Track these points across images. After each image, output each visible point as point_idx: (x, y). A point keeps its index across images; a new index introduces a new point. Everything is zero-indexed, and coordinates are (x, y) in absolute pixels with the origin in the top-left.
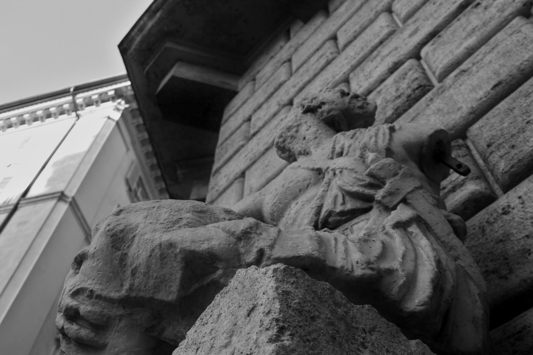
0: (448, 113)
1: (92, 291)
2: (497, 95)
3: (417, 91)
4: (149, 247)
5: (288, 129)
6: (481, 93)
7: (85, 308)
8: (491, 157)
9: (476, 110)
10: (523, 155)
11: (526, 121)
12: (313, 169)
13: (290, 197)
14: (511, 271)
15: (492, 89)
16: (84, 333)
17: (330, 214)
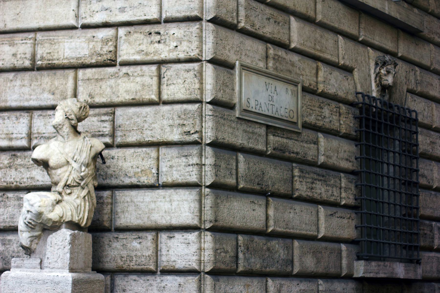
0: (114, 93)
3: (109, 61)
7: (33, 223)
14: (106, 179)
16: (32, 227)
17: (70, 184)
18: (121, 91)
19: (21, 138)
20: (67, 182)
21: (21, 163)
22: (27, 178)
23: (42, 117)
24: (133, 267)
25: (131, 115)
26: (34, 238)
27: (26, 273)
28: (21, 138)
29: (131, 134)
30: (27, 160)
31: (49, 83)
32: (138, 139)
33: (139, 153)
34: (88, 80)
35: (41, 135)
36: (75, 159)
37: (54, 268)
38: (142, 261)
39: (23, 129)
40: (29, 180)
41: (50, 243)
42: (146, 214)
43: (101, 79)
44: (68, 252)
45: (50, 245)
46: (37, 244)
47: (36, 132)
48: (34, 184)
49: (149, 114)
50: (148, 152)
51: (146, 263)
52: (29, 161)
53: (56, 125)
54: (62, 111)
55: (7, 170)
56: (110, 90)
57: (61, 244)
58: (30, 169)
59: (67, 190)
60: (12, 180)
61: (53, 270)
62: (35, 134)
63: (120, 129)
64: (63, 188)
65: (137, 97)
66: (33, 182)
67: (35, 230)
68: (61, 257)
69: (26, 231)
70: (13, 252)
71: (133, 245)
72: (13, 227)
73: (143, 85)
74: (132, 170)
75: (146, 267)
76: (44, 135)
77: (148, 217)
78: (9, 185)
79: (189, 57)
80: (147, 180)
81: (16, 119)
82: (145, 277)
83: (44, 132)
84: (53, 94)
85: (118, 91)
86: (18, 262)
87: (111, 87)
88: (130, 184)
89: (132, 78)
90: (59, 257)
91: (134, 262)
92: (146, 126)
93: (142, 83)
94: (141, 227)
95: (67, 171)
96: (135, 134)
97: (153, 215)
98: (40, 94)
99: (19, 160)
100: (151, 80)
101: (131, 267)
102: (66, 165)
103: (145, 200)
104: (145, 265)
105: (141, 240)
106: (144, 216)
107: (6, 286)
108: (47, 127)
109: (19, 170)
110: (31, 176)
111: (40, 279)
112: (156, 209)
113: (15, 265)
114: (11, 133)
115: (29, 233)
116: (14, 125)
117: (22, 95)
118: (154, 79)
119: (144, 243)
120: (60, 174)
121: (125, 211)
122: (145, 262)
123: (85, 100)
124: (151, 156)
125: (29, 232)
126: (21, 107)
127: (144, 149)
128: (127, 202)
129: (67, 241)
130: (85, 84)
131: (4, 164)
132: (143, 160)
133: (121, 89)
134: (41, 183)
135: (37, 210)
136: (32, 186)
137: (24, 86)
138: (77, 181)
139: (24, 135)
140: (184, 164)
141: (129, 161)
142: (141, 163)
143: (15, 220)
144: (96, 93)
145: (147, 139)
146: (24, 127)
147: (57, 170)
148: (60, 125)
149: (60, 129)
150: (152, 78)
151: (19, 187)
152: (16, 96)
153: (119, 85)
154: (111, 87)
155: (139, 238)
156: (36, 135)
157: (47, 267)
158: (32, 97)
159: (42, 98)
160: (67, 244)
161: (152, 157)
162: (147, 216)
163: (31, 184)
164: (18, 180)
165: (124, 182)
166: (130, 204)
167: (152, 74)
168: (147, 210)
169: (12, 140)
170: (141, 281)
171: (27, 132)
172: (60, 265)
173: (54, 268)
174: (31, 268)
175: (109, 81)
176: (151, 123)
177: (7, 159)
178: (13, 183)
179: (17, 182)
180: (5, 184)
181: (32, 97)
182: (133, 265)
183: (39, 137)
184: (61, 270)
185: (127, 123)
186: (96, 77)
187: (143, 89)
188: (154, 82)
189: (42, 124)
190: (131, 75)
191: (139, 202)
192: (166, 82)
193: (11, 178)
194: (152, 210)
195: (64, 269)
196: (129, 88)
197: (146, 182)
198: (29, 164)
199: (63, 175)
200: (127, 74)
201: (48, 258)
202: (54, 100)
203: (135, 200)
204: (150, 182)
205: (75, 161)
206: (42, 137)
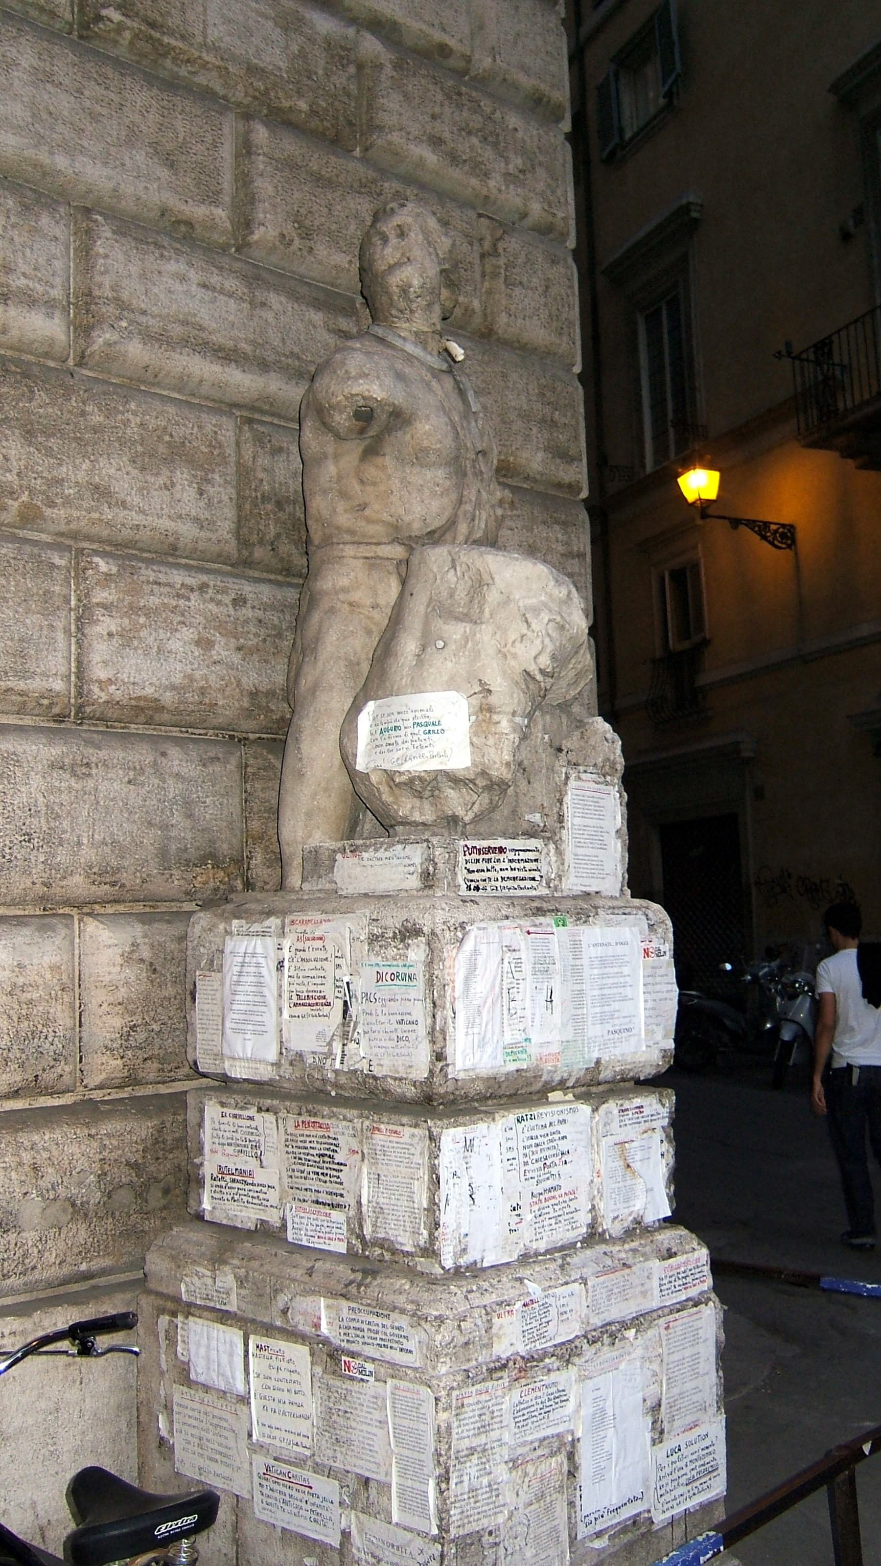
43: (329, 181)
79: (550, 218)
84: (172, 165)
117: (45, 116)
139: (56, 293)
140: (561, 548)
143: (32, 666)
179: (32, 491)
189: (134, 269)
192: (503, 271)
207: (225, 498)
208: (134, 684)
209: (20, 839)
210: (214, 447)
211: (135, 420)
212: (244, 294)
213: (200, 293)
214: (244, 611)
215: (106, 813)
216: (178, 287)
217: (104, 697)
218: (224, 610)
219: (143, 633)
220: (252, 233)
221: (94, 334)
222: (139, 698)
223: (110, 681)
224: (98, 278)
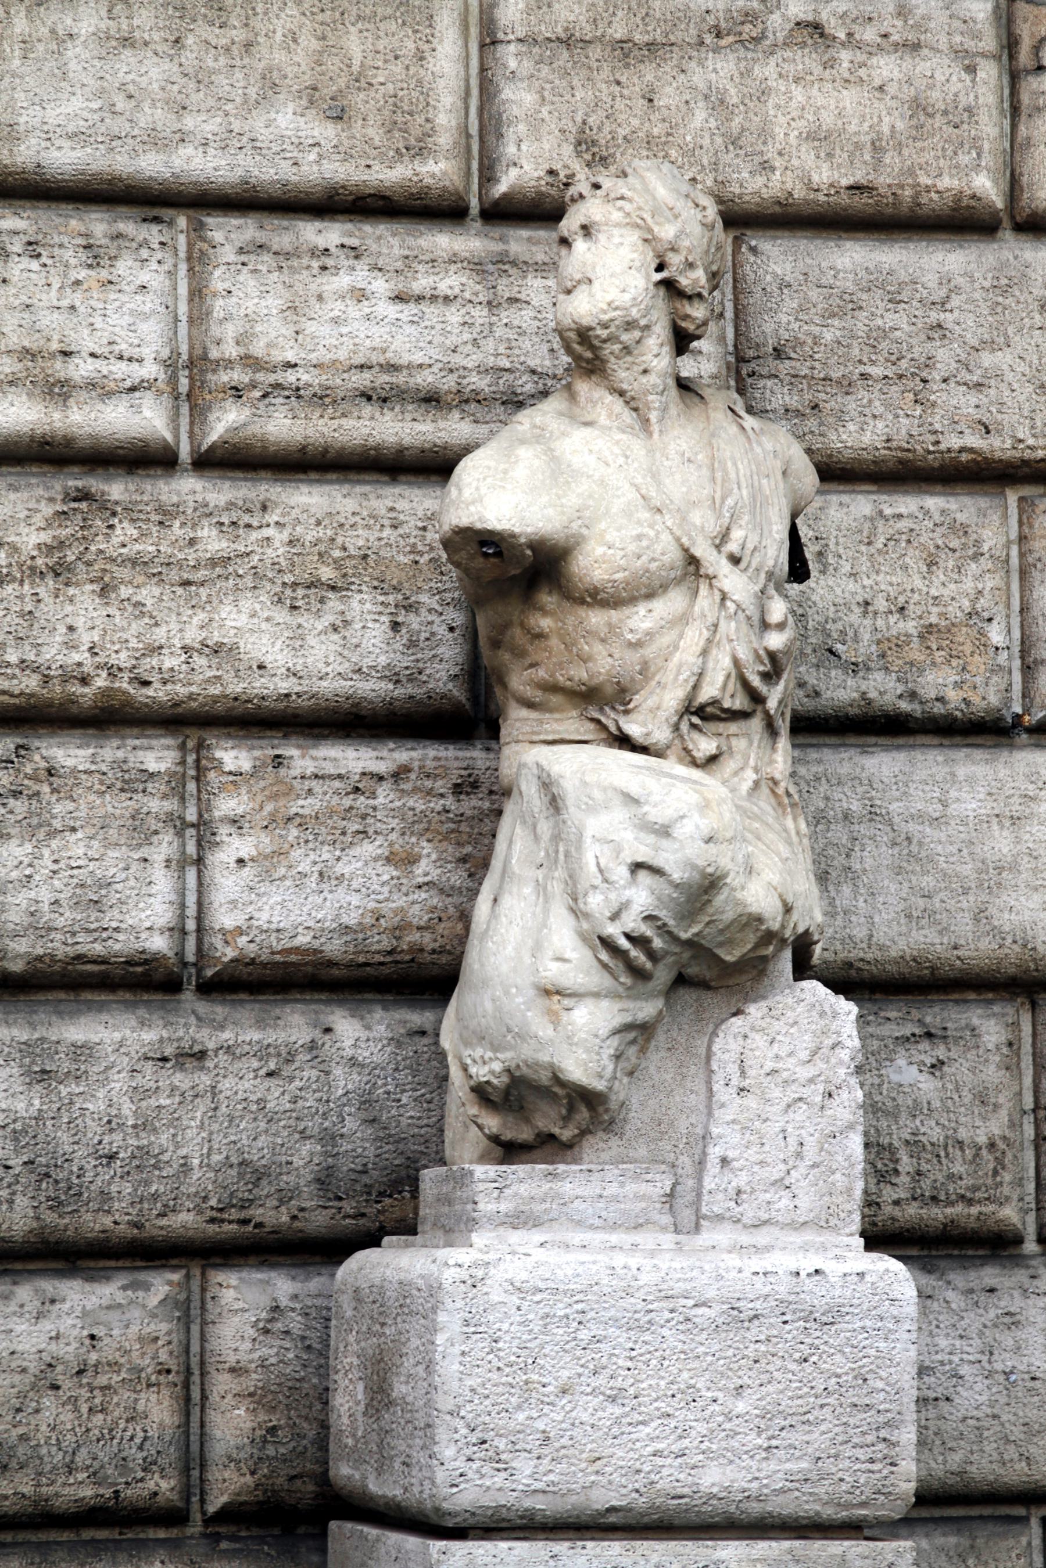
1: (665, 925)
2: (845, 210)
4: (739, 910)
5: (628, 323)
6: (823, 175)
7: (658, 943)
8: (769, 383)
9: (791, 205)
10: (820, 446)
11: (862, 369)
12: (686, 550)
13: (644, 591)
15: (850, 188)
16: (649, 965)
17: (715, 702)
18: (779, 132)
19: (133, 389)
20: (696, 687)
21: (138, 547)
22: (186, 649)
23: (266, 257)
24: (897, 1212)
25: (851, 287)
26: (631, 1035)
27: (603, 1258)
28: (133, 389)
29: (851, 405)
30: (177, 529)
31: (309, 42)
32: (900, 439)
33: (903, 525)
34: (567, 41)
35: (272, 378)
36: (732, 547)
37: (766, 1222)
38: (951, 1177)
39: (144, 327)
40: (200, 661)
41: (733, 1069)
42: (966, 892)
43: (650, 45)
44: (851, 1127)
45: (735, 1082)
46: (631, 1074)
47: (231, 350)
48: (236, 687)
49: (957, 290)
50: (961, 518)
51: (975, 1189)
52: (192, 542)
53: (605, 326)
54: (634, 237)
55: (42, 591)
56: (713, 124)
57: (804, 1073)
58: (204, 592)
59: (696, 735)
60: (81, 656)
61: (762, 1237)
62: (229, 364)
63: (784, 367)
64: (676, 728)
65: (883, 180)
66: (229, 677)
67: (651, 985)
68: (811, 1153)
69: (596, 995)
70: (111, 1125)
71: (895, 1078)
72: (102, 961)
73: (919, 107)
74: (868, 622)
75: (974, 1210)
76: (290, 377)
77: (980, 915)
78: (58, 688)
80: (958, 685)
81: (83, 255)
82: (973, 1274)
83: (290, 356)
84: (339, 117)
85: (765, 134)
86: (523, 1189)
87: (718, 103)
88: (853, 711)
89: (845, 56)
90: (799, 1155)
91: (903, 1179)
92: (945, 357)
93: (909, 92)
94: (933, 969)
95: (683, 620)
96: (878, 408)
97: (1008, 898)
98: (249, 106)
99: (123, 530)
100: (967, 78)
101: (888, 1210)
102: (678, 581)
103: (954, 809)
104: (970, 1202)
105: (941, 1052)
106: (951, 904)
107: (479, 1347)
108: (311, 327)
109: (125, 592)
110: (216, 637)
111: (711, 1294)
112: (1025, 863)
113: (503, 1207)
114: (55, 346)
115: (618, 1005)
116: (76, 298)
118: (981, 75)
119: (961, 1069)
120: (650, 634)
121: (834, 874)
122: (967, 1182)
123: (551, 172)
124: (977, 543)
125: (613, 995)
126: (114, 180)
127: (934, 502)
128: (846, 816)
129: (844, 1055)
130: (545, 70)
131: (15, 549)
132: (931, 564)
133: (782, 120)
134: (284, 686)
135: (701, 863)
136: (215, 699)
137: (127, 41)
138: (756, 681)
139: (150, 370)
141: (846, 568)
142: (918, 583)
143: (111, 918)
144: (621, 132)
145: (953, 442)
146: (145, 317)
147: (627, 611)
148: (630, 325)
149: (627, 350)
150: (971, 70)
151: (128, 702)
152: (77, 104)
153: (764, 93)
154: (718, 103)
155: (929, 1035)
156: (238, 376)
157: (720, 1218)
158: (189, 122)
159: (264, 135)
160: (842, 1071)
161: (985, 548)
162: (968, 902)
163: (215, 690)
164: (123, 659)
165: (817, 694)
166: (863, 829)
167: (970, 44)
168: (967, 870)
169: (65, 397)
170: (950, 1295)
171: (165, 353)
172: (805, 1202)
173: (766, 1222)
174: (615, 1226)
175: (701, 64)
176: (975, 342)
177: (38, 520)
178: (84, 681)
179: (113, 672)
180: (31, 683)
181: (189, 122)
182: (897, 1203)
183: (253, 385)
184: (809, 1236)
185: (828, 336)
186: (619, 32)
187: (918, 132)
188: (981, 90)
189: (273, 303)
190: (842, 35)
191: (920, 817)
193: (71, 646)
194: (1000, 870)
195: (835, 1229)
196: (828, 120)
197: (954, 696)
198: (192, 556)
199: (665, 640)
200: (816, 28)
201: (724, 1161)
202: (347, 157)
203: (894, 806)
204: (976, 699)
205: (735, 560)
206: (278, 386)
207: (442, 630)
208: (278, 931)
209: (94, 1163)
210: (421, 554)
211: (280, 537)
212: (476, 294)
213: (392, 311)
214: (475, 802)
215: (231, 1121)
216: (354, 311)
217: (230, 953)
218: (438, 805)
219: (296, 853)
220: (498, 181)
221: (212, 417)
222: (288, 951)
223: (239, 931)
224: (216, 331)
